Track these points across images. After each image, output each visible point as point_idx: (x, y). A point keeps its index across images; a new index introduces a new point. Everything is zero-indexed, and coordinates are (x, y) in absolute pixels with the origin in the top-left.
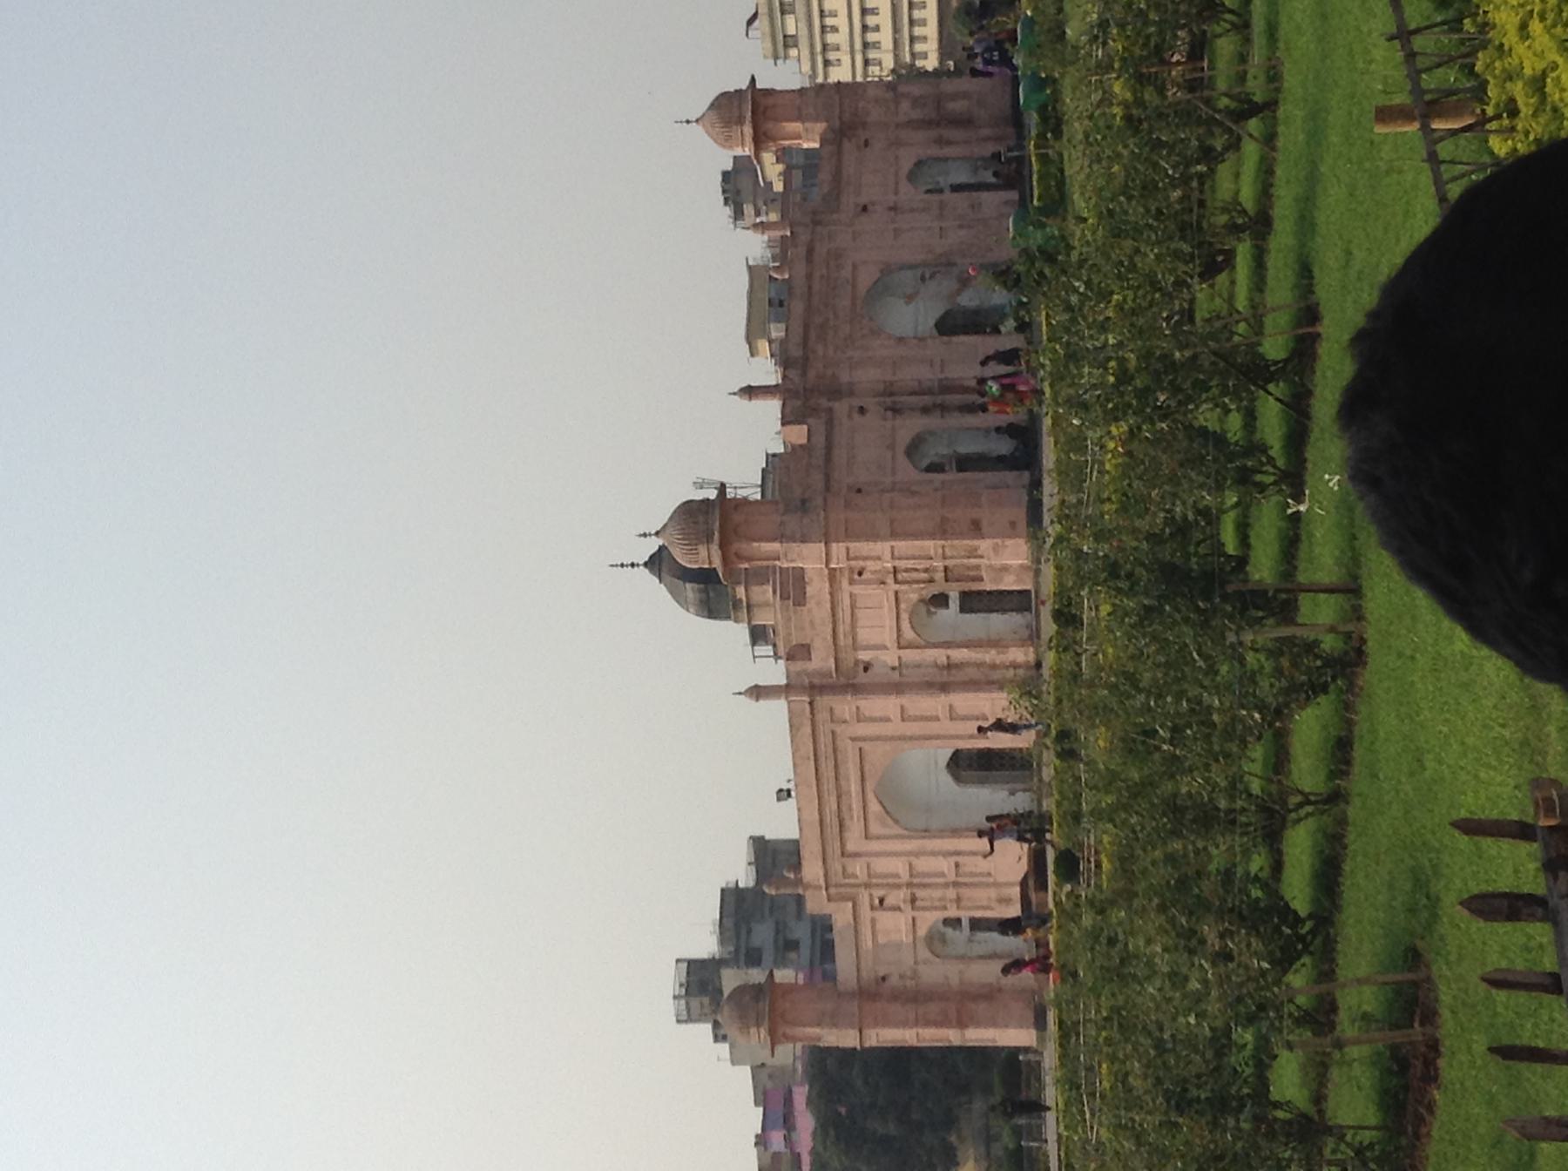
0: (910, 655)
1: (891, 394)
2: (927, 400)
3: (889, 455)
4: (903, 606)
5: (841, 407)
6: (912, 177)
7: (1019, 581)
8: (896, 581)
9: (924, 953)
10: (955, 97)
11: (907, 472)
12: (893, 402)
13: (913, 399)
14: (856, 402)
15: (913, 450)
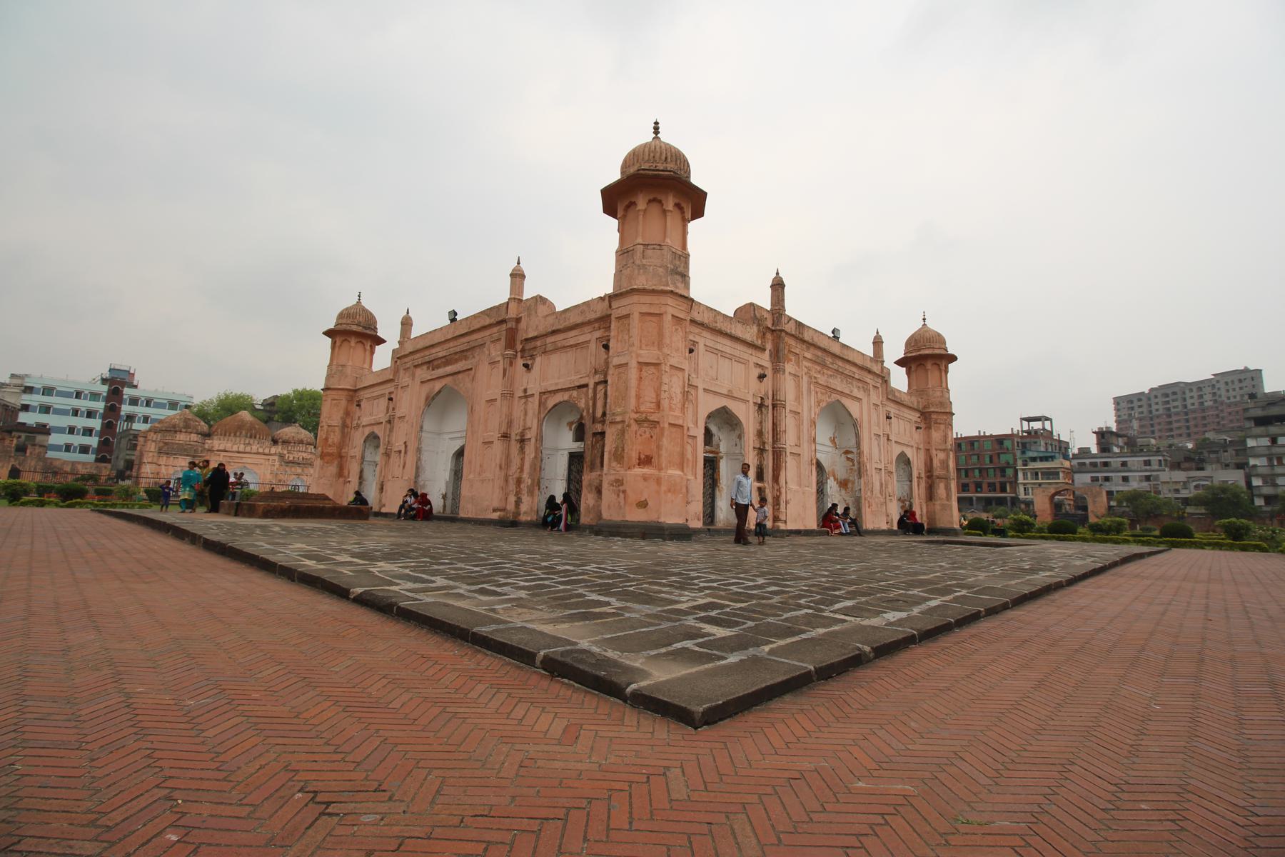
0: (533, 404)
1: (774, 406)
2: (769, 438)
3: (725, 392)
4: (575, 393)
5: (765, 359)
6: (902, 455)
7: (588, 508)
8: (597, 384)
9: (367, 431)
10: (948, 488)
11: (709, 404)
12: (770, 406)
13: (768, 426)
14: (769, 373)
15: (725, 418)
